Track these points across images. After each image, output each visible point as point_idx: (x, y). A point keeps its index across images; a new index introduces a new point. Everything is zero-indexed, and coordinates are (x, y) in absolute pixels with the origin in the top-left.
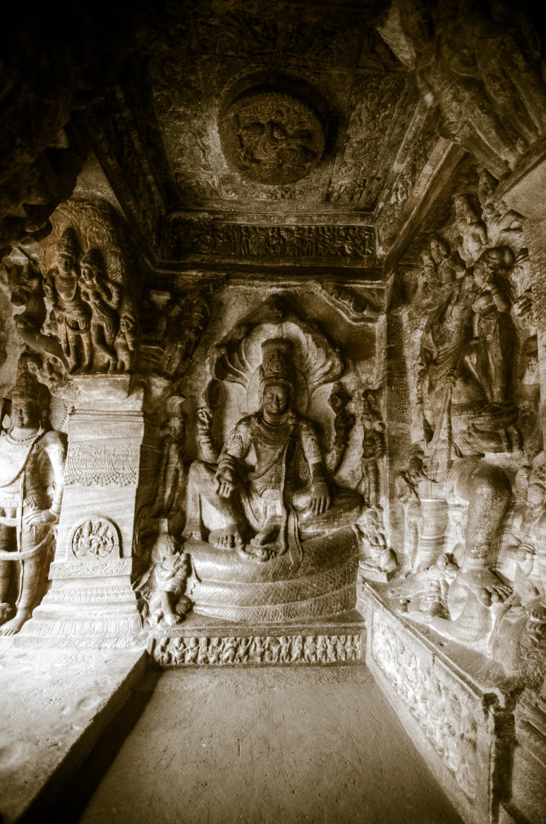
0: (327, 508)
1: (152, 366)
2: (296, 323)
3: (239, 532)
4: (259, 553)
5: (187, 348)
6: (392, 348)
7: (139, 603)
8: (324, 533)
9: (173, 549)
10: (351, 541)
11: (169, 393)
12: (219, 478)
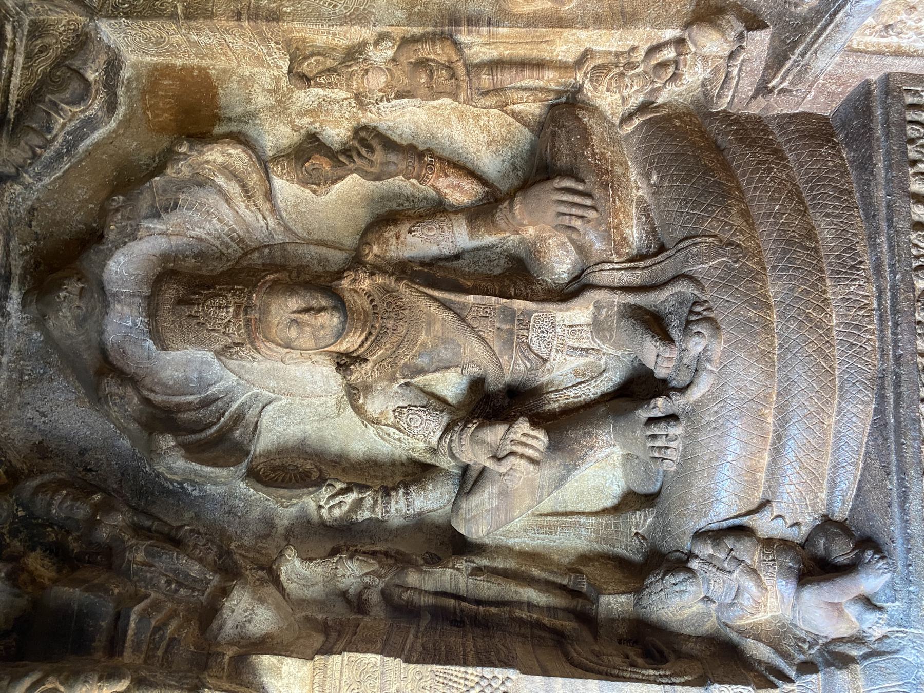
0: (580, 187)
1: (190, 633)
2: (109, 255)
3: (636, 409)
4: (696, 346)
5: (150, 538)
6: (186, 8)
7: (829, 664)
8: (641, 200)
9: (681, 577)
10: (663, 129)
11: (271, 590)
12: (498, 459)
